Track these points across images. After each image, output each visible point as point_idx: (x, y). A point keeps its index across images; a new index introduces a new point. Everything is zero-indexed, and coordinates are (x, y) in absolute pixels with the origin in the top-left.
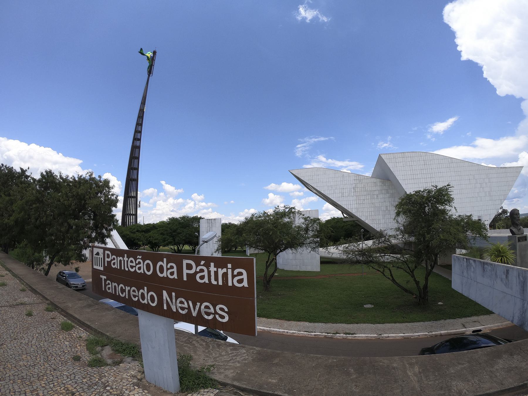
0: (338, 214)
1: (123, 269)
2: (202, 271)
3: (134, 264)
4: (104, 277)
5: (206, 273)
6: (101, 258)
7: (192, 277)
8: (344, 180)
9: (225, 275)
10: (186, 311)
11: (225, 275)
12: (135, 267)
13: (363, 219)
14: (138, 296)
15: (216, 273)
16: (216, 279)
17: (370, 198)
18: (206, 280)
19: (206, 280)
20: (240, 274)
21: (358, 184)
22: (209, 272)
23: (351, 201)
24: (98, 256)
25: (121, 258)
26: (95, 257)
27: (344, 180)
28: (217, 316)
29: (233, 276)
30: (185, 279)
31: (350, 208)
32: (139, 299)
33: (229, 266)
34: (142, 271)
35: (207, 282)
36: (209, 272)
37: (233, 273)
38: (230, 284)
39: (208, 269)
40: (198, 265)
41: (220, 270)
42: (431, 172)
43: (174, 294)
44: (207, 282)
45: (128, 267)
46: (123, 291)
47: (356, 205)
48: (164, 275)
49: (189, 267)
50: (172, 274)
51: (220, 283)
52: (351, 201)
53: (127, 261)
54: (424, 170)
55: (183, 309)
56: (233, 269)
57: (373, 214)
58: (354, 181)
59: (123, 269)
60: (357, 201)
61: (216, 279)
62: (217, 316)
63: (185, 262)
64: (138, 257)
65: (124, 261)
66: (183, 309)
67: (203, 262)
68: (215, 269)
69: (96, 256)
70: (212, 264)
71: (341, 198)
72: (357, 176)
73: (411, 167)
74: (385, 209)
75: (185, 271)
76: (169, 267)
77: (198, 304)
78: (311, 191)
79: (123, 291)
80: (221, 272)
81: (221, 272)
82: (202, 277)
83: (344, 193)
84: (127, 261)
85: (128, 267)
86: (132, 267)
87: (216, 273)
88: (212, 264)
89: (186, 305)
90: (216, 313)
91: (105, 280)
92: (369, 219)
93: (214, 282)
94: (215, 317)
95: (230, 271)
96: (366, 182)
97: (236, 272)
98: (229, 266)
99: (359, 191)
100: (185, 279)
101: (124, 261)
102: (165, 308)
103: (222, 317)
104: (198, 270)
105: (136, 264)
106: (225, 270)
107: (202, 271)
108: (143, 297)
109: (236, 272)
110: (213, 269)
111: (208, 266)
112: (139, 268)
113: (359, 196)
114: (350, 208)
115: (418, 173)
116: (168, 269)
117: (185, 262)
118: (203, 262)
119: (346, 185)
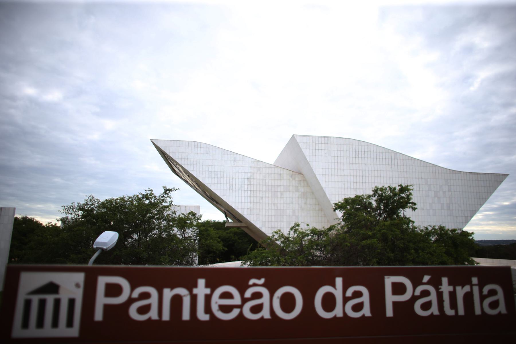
0: (218, 216)
1: (186, 316)
2: (426, 293)
5: (433, 297)
6: (72, 302)
8: (235, 165)
11: (468, 297)
12: (241, 307)
13: (258, 225)
15: (453, 295)
16: (454, 305)
17: (270, 195)
18: (434, 310)
19: (434, 310)
21: (255, 174)
22: (440, 295)
23: (243, 198)
24: (50, 299)
25: (182, 291)
26: (28, 303)
27: (235, 165)
29: (483, 298)
30: (389, 312)
31: (240, 207)
33: (475, 280)
34: (266, 313)
35: (436, 312)
36: (440, 295)
37: (481, 291)
41: (458, 289)
42: (364, 169)
44: (436, 312)
45: (208, 309)
47: (249, 204)
48: (338, 312)
49: (399, 289)
50: (358, 308)
51: (461, 312)
52: (243, 198)
53: (208, 298)
54: (354, 165)
56: (481, 286)
57: (273, 220)
58: (250, 168)
60: (252, 199)
61: (454, 305)
63: (389, 281)
65: (194, 299)
67: (426, 278)
68: (451, 288)
70: (445, 280)
71: (228, 191)
72: (255, 162)
73: (336, 158)
74: (291, 214)
75: (390, 298)
76: (349, 293)
78: (178, 175)
80: (461, 292)
81: (461, 292)
82: (426, 306)
83: (234, 186)
84: (208, 298)
85: (208, 309)
86: (226, 309)
87: (453, 295)
88: (445, 280)
92: (267, 226)
93: (449, 312)
95: (476, 289)
96: (267, 172)
98: (475, 280)
99: (255, 184)
100: (389, 312)
104: (418, 292)
105: (245, 301)
106: (467, 288)
107: (426, 293)
110: (446, 288)
111: (436, 283)
112: (257, 309)
113: (255, 192)
114: (240, 207)
115: (345, 168)
116: (346, 300)
117: (389, 281)
118: (426, 278)
119: (237, 173)
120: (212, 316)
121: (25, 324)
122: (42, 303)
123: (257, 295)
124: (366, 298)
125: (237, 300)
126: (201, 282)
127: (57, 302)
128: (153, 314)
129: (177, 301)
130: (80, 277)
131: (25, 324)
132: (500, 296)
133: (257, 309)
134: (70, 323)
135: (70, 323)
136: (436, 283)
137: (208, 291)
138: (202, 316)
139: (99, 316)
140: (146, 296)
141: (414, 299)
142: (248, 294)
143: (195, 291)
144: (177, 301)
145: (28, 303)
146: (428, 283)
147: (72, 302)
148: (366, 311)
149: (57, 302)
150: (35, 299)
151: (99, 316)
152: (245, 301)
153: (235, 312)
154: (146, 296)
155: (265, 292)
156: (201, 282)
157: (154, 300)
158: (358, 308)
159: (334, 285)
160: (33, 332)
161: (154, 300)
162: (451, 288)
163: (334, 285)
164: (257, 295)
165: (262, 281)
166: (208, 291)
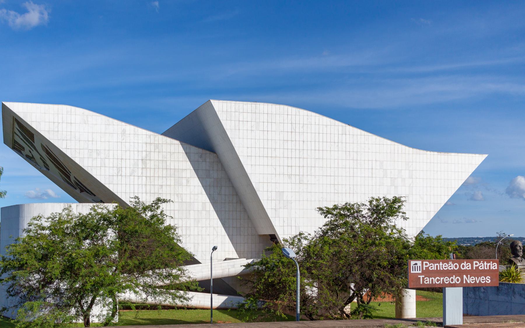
1: (439, 269)
2: (481, 265)
3: (447, 266)
4: (421, 277)
5: (483, 266)
6: (420, 266)
7: (477, 268)
9: (490, 266)
10: (474, 281)
11: (490, 266)
14: (449, 281)
15: (487, 265)
16: (487, 267)
18: (483, 268)
20: (495, 265)
22: (484, 265)
24: (416, 266)
25: (438, 264)
26: (413, 267)
28: (486, 281)
29: (492, 266)
32: (449, 282)
33: (491, 262)
34: (452, 268)
35: (483, 269)
36: (484, 265)
38: (491, 269)
39: (484, 264)
40: (480, 263)
41: (488, 264)
43: (469, 276)
44: (483, 269)
45: (442, 268)
46: (438, 280)
48: (465, 268)
49: (476, 264)
50: (468, 267)
51: (488, 269)
53: (442, 265)
55: (473, 281)
56: (492, 263)
59: (439, 269)
61: (487, 267)
62: (486, 281)
63: (475, 262)
64: (450, 262)
65: (440, 265)
66: (473, 281)
68: (486, 264)
69: (414, 266)
70: (485, 262)
75: (475, 266)
76: (467, 265)
77: (480, 278)
79: (438, 280)
80: (488, 264)
82: (481, 267)
84: (442, 265)
85: (442, 268)
86: (445, 268)
87: (487, 265)
88: (485, 262)
89: (474, 279)
90: (486, 280)
91: (423, 278)
93: (486, 269)
94: (486, 282)
95: (491, 264)
97: (493, 264)
98: (491, 262)
101: (440, 265)
102: (464, 282)
103: (488, 281)
104: (480, 265)
106: (490, 264)
107: (481, 265)
108: (452, 280)
109: (493, 264)
110: (485, 264)
111: (483, 263)
112: (451, 268)
116: (466, 266)
117: (475, 262)
120: (443, 269)
121: (413, 271)
122: (415, 267)
123: (451, 265)
124: (470, 266)
125: (447, 266)
126: (441, 263)
127: (417, 266)
128: (433, 269)
129: (437, 266)
130: (421, 262)
131: (413, 271)
132: (496, 266)
133: (451, 268)
134: (420, 270)
135: (420, 270)
136: (483, 263)
137: (442, 264)
138: (442, 269)
139: (424, 269)
140: (432, 265)
141: (479, 266)
142: (449, 265)
143: (440, 264)
144: (437, 266)
145: (413, 267)
146: (482, 263)
147: (420, 266)
148: (470, 268)
149: (417, 266)
150: (414, 266)
151: (424, 269)
152: (448, 266)
153: (447, 268)
154: (432, 265)
155: (452, 264)
156: (441, 263)
157: (433, 266)
158: (468, 267)
159: (464, 263)
160: (414, 272)
161: (433, 266)
162: (486, 264)
163: (464, 263)
164: (451, 265)
165: (451, 262)
166: (442, 264)
